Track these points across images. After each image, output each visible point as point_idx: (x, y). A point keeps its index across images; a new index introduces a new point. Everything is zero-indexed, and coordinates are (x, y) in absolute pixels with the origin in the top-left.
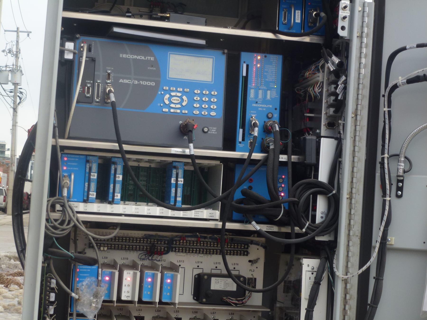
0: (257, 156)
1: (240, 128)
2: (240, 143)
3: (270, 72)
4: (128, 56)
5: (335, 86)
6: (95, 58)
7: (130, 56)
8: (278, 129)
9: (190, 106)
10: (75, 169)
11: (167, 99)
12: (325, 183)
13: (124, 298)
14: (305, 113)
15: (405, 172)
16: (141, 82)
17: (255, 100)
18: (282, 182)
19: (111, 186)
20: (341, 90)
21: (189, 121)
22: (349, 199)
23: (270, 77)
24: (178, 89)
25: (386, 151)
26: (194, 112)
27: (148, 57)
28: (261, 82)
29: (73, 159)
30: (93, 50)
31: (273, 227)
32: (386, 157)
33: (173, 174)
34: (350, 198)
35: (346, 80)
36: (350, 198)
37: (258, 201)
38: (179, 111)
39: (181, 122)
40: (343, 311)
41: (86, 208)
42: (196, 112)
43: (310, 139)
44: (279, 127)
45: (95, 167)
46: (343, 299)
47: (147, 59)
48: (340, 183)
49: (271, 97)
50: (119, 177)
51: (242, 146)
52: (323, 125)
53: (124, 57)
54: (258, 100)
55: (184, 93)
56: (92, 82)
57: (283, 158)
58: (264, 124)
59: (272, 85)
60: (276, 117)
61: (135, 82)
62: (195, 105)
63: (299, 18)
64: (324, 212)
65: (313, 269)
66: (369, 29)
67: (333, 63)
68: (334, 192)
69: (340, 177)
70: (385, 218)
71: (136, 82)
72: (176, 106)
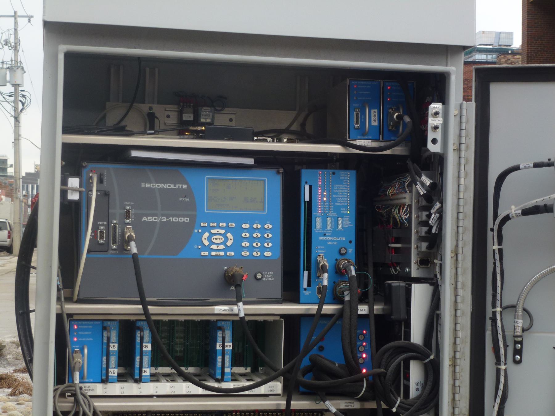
0: (328, 309)
1: (304, 270)
2: (305, 289)
4: (153, 186)
5: (427, 213)
6: (109, 192)
7: (155, 186)
8: (354, 273)
9: (237, 247)
10: (89, 339)
11: (206, 239)
12: (418, 344)
14: (390, 244)
15: (524, 330)
16: (171, 218)
17: (322, 231)
18: (362, 339)
19: (138, 359)
20: (435, 222)
21: (236, 270)
22: (451, 366)
24: (221, 225)
25: (498, 303)
26: (243, 254)
27: (179, 185)
28: (330, 205)
29: (85, 327)
30: (105, 180)
31: (353, 403)
32: (498, 311)
33: (218, 338)
34: (454, 364)
35: (441, 207)
36: (454, 365)
37: (333, 375)
38: (222, 254)
39: (226, 268)
41: (105, 390)
43: (397, 287)
44: (356, 270)
45: (114, 335)
47: (177, 187)
48: (439, 344)
49: (344, 227)
50: (147, 347)
51: (308, 294)
52: (414, 262)
53: (147, 187)
54: (326, 231)
55: (228, 229)
56: (106, 223)
57: (363, 309)
58: (337, 262)
59: (345, 211)
60: (351, 252)
61: (163, 219)
62: (243, 244)
63: (376, 119)
64: (420, 382)
66: (469, 139)
67: (423, 184)
68: (432, 357)
69: (439, 336)
70: (500, 393)
71: (165, 219)
72: (218, 247)
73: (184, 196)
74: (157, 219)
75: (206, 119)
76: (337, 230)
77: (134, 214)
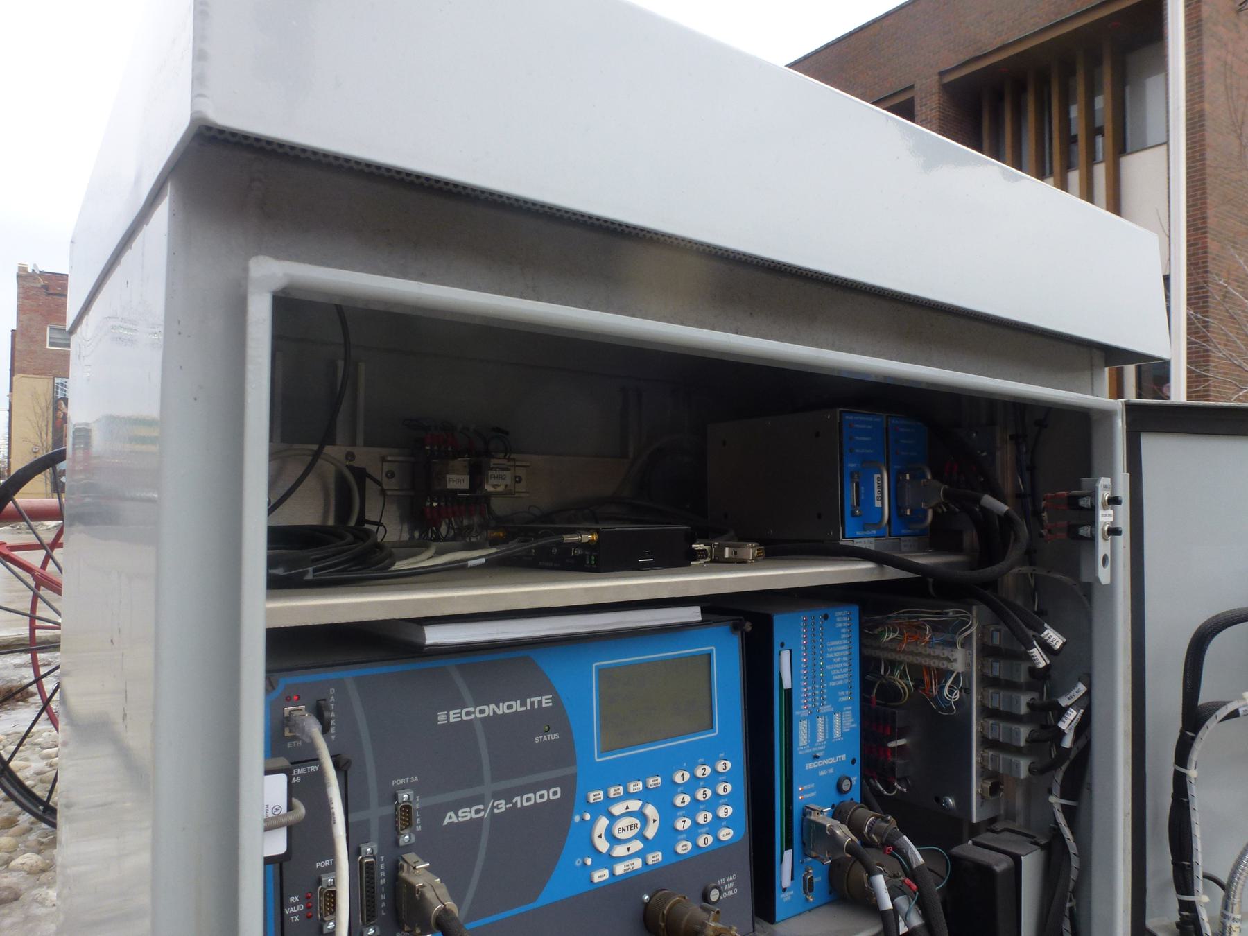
2: (784, 890)
3: (838, 659)
4: (468, 714)
7: (474, 713)
11: (603, 836)
16: (518, 799)
23: (838, 674)
27: (532, 699)
35: (1088, 693)
38: (638, 863)
42: (685, 845)
47: (529, 708)
51: (789, 898)
53: (452, 720)
55: (646, 796)
61: (497, 807)
71: (502, 806)
73: (547, 727)
74: (483, 810)
75: (494, 486)
76: (833, 740)
77: (421, 810)
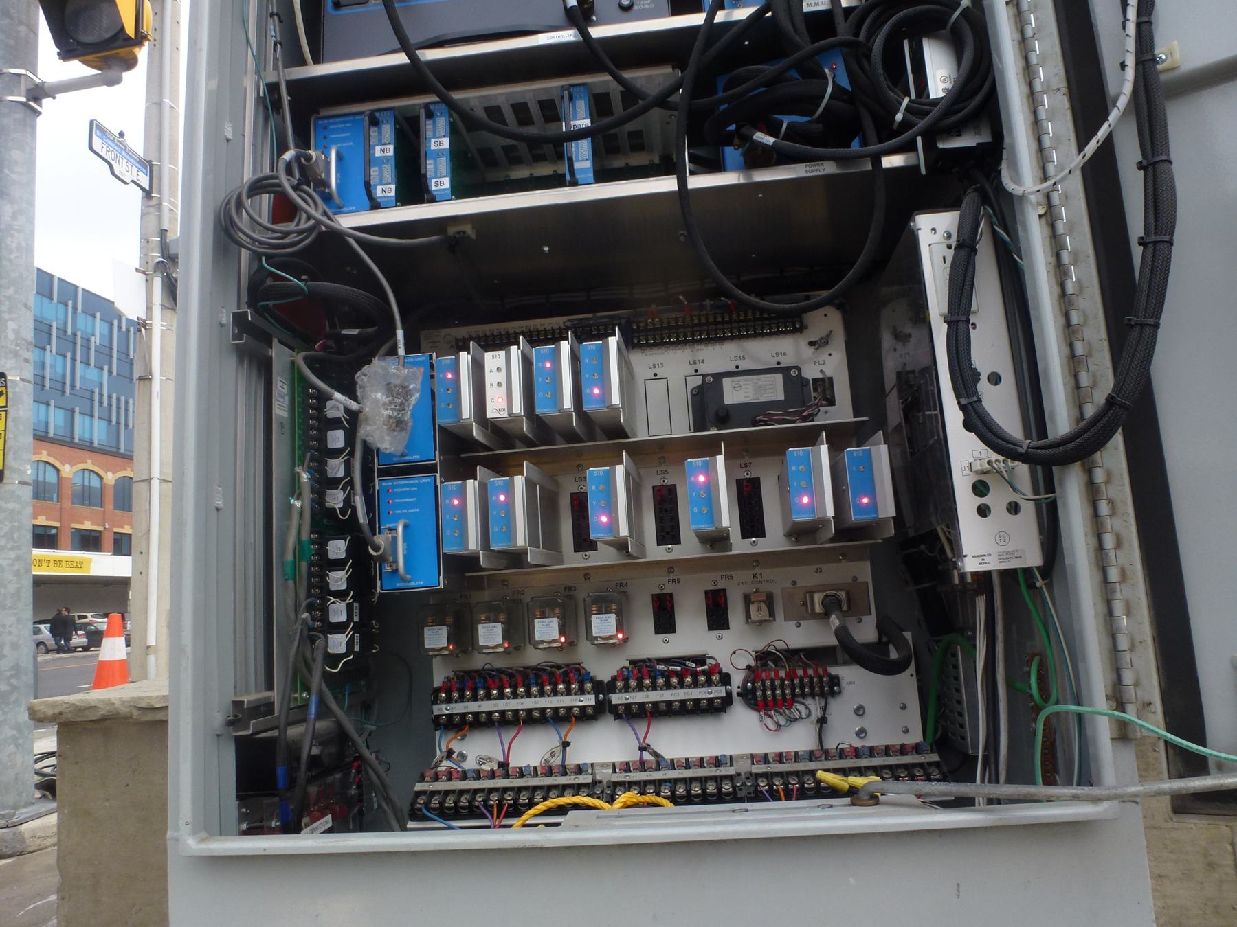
13: (491, 414)
29: (340, 126)
31: (822, 164)
40: (1060, 304)
45: (388, 130)
46: (1051, 268)
65: (949, 236)
